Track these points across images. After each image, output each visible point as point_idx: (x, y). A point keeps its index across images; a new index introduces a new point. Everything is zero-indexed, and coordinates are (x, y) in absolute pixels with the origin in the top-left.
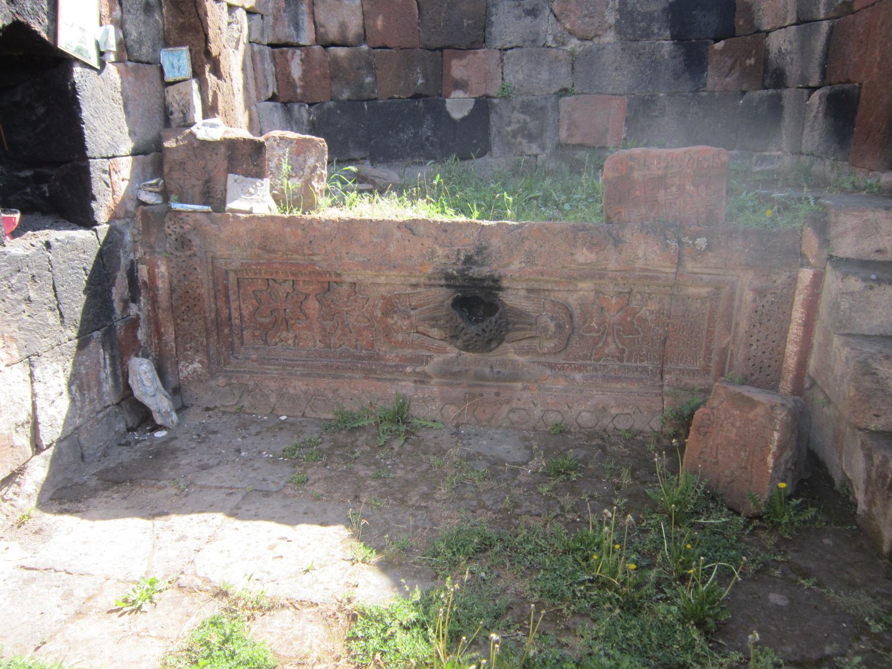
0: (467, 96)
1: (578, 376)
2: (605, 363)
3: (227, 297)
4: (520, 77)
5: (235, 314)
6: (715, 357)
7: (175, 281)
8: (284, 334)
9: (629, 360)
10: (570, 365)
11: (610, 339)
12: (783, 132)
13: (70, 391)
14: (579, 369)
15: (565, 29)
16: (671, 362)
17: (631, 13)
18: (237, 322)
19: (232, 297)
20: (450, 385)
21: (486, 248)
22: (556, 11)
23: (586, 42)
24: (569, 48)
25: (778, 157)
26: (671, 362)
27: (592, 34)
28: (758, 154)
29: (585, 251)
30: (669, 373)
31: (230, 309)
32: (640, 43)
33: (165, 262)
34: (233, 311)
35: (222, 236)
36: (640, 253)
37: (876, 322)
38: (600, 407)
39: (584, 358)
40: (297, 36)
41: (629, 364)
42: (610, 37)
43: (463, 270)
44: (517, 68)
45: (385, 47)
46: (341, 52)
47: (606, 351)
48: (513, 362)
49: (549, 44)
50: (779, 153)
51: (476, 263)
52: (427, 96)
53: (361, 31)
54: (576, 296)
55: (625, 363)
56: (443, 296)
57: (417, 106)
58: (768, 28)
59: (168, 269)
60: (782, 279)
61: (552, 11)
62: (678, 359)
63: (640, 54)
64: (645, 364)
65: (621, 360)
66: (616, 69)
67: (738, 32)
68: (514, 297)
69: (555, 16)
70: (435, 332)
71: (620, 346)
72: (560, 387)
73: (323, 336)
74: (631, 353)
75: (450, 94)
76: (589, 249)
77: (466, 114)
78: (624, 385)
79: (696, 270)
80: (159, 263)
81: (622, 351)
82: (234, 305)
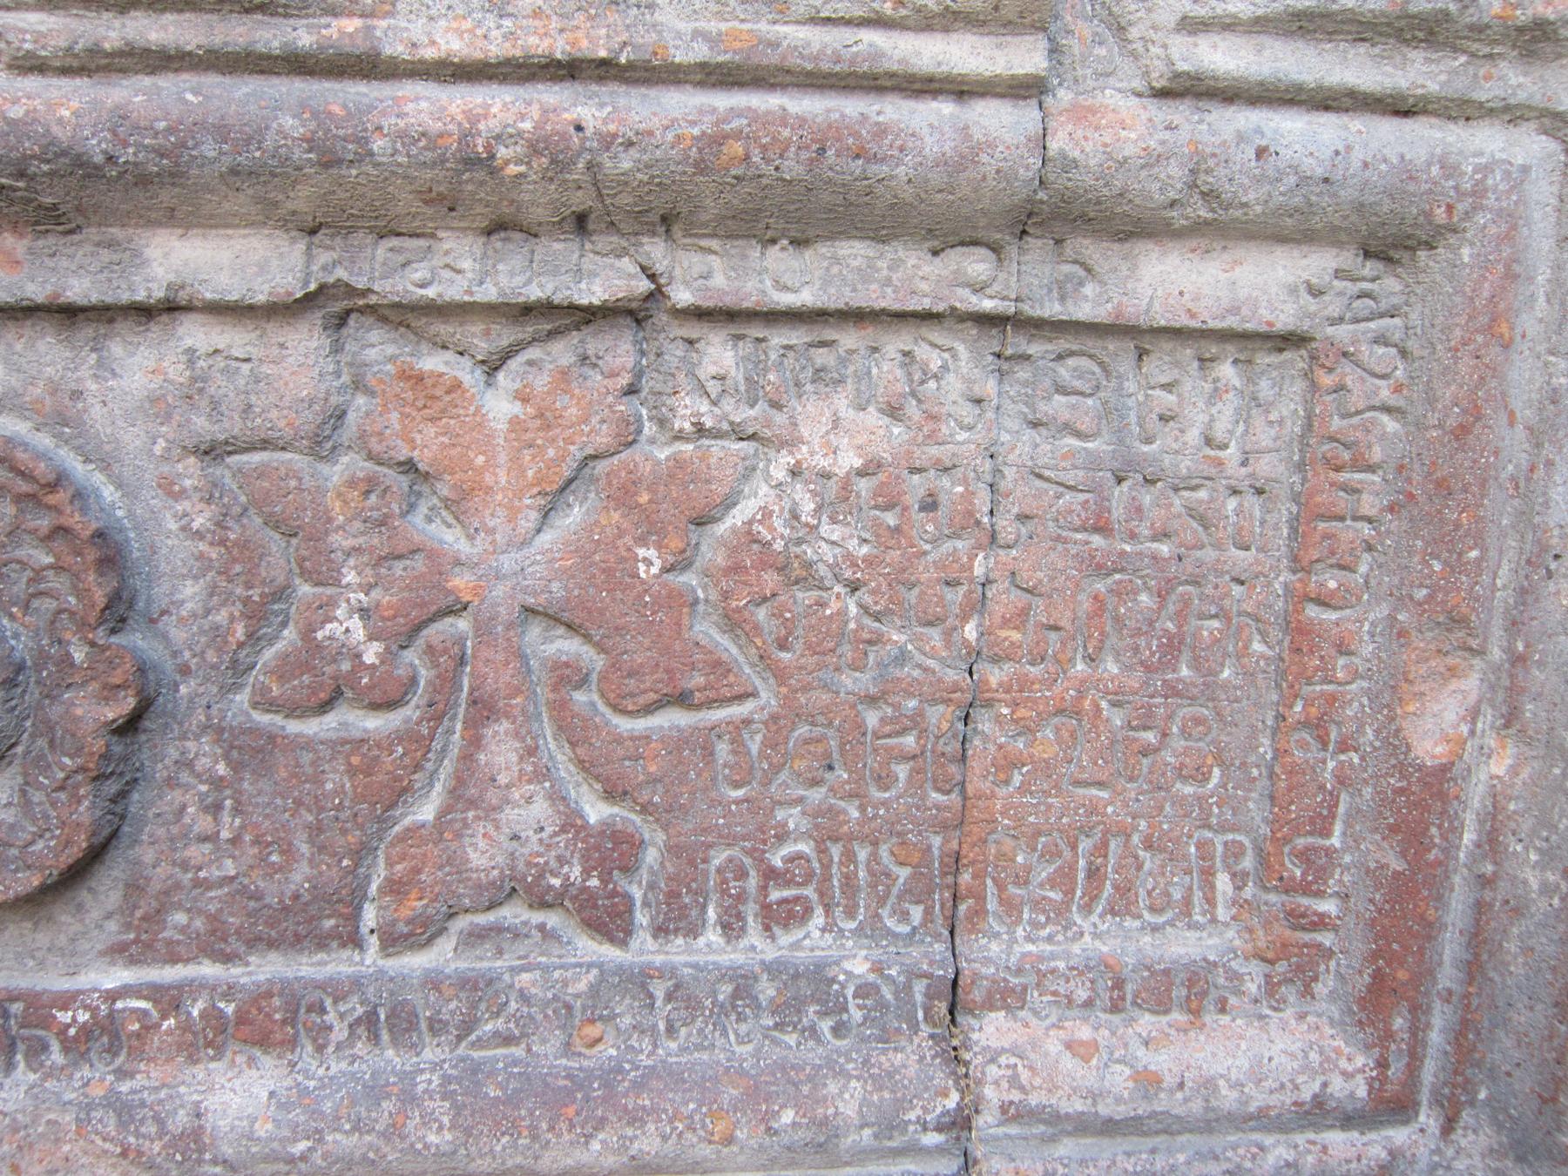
2: (483, 961)
6: (1356, 849)
9: (676, 920)
10: (169, 999)
11: (501, 752)
14: (266, 1026)
16: (1011, 908)
26: (1011, 908)
30: (1006, 997)
39: (297, 926)
41: (677, 952)
47: (482, 855)
54: (142, 364)
62: (1064, 879)
65: (609, 920)
71: (596, 811)
74: (687, 855)
79: (1222, 57)
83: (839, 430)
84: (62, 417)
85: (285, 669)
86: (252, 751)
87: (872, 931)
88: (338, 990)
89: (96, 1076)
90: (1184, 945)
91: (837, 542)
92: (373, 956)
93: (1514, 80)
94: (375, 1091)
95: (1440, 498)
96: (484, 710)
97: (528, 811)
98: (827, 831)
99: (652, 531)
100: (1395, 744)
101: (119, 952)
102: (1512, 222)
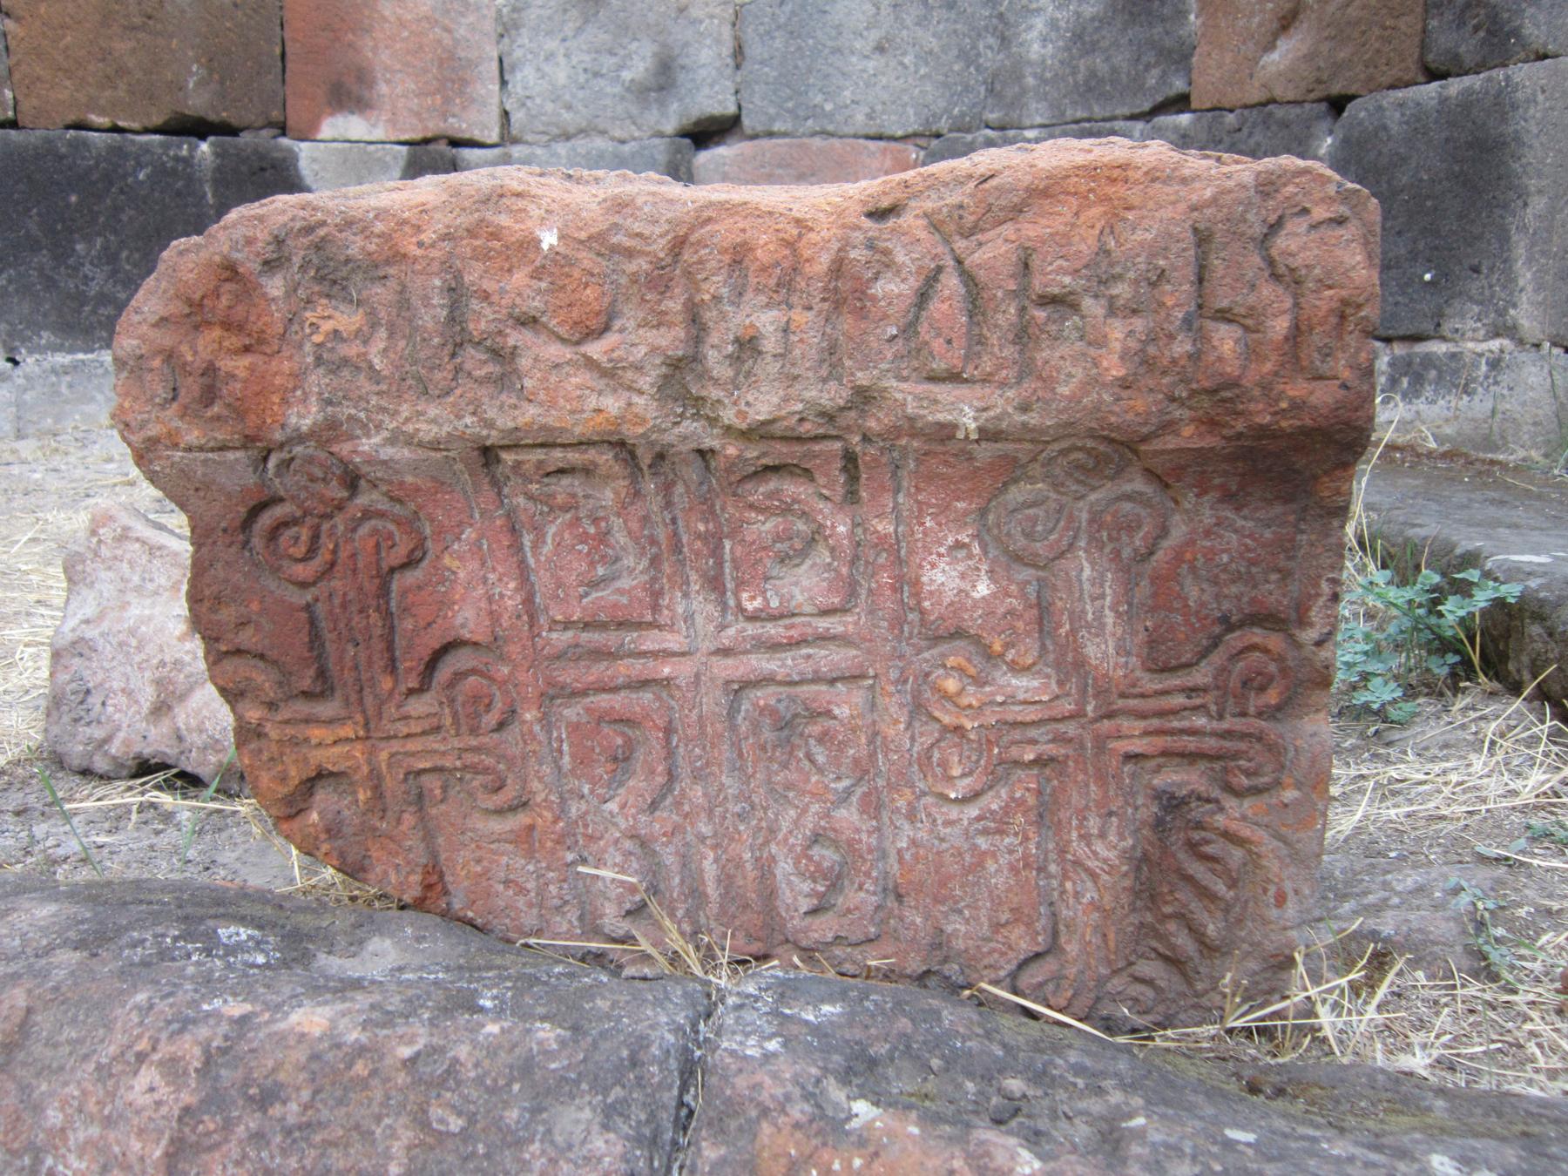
0: (379, 134)
4: (561, 77)
12: (1520, 251)
25: (1495, 364)
28: (1399, 349)
44: (552, 44)
50: (1495, 344)
52: (231, 130)
57: (187, 161)
66: (880, 49)
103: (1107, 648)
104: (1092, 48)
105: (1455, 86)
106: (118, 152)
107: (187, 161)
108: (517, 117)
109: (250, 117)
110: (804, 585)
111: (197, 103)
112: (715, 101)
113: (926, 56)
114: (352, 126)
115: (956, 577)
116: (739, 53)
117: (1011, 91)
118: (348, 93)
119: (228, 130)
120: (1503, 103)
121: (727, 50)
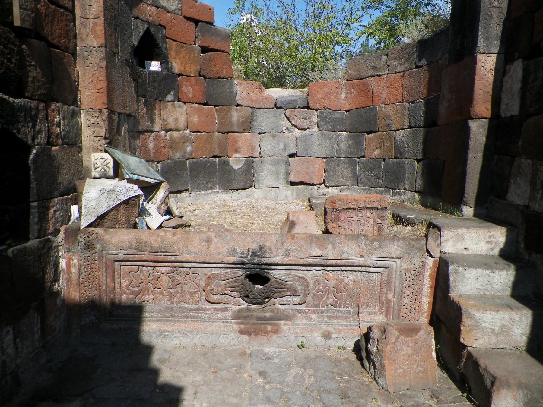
1: (314, 316)
3: (113, 276)
4: (269, 148)
5: (117, 286)
7: (82, 268)
8: (147, 297)
9: (340, 307)
10: (309, 310)
11: (330, 296)
13: (15, 343)
14: (314, 312)
15: (292, 125)
17: (326, 118)
18: (119, 290)
19: (116, 277)
20: (242, 323)
21: (263, 248)
22: (287, 115)
23: (303, 131)
24: (294, 134)
27: (306, 127)
29: (316, 249)
31: (114, 283)
32: (331, 132)
33: (77, 257)
34: (116, 284)
35: (113, 242)
36: (345, 250)
37: (469, 288)
38: (327, 333)
40: (152, 127)
41: (340, 309)
42: (315, 129)
43: (251, 260)
44: (268, 143)
45: (199, 132)
46: (176, 134)
47: (328, 302)
48: (278, 310)
49: (284, 131)
51: (257, 256)
53: (186, 123)
55: (338, 309)
56: (238, 272)
58: (395, 129)
59: (78, 261)
60: (418, 263)
61: (285, 115)
62: (366, 306)
63: (331, 138)
64: (349, 309)
65: (335, 307)
67: (380, 129)
68: (278, 274)
69: (287, 118)
70: (235, 294)
72: (304, 323)
73: (170, 297)
74: (341, 303)
75: (232, 155)
76: (319, 248)
77: (241, 166)
78: (339, 321)
79: (374, 259)
80: (73, 258)
81: (336, 302)
82: (117, 281)
83: (352, 277)
84: (306, 275)
85: (317, 290)
86: (315, 295)
87: (353, 308)
88: (319, 310)
89: (305, 315)
90: (374, 310)
91: (351, 283)
92: (321, 308)
93: (392, 260)
94: (322, 316)
95: (389, 283)
96: (329, 293)
97: (332, 299)
98: (350, 301)
99: (340, 282)
100: (387, 298)
101: (306, 307)
102: (392, 267)
103: (376, 218)
104: (351, 148)
105: (398, 160)
106: (206, 161)
107: (215, 162)
108: (262, 154)
109: (223, 155)
110: (361, 215)
111: (216, 154)
112: (293, 151)
113: (326, 147)
114: (238, 155)
115: (369, 214)
116: (297, 145)
117: (339, 152)
118: (236, 151)
119: (220, 157)
120: (403, 163)
121: (295, 143)
